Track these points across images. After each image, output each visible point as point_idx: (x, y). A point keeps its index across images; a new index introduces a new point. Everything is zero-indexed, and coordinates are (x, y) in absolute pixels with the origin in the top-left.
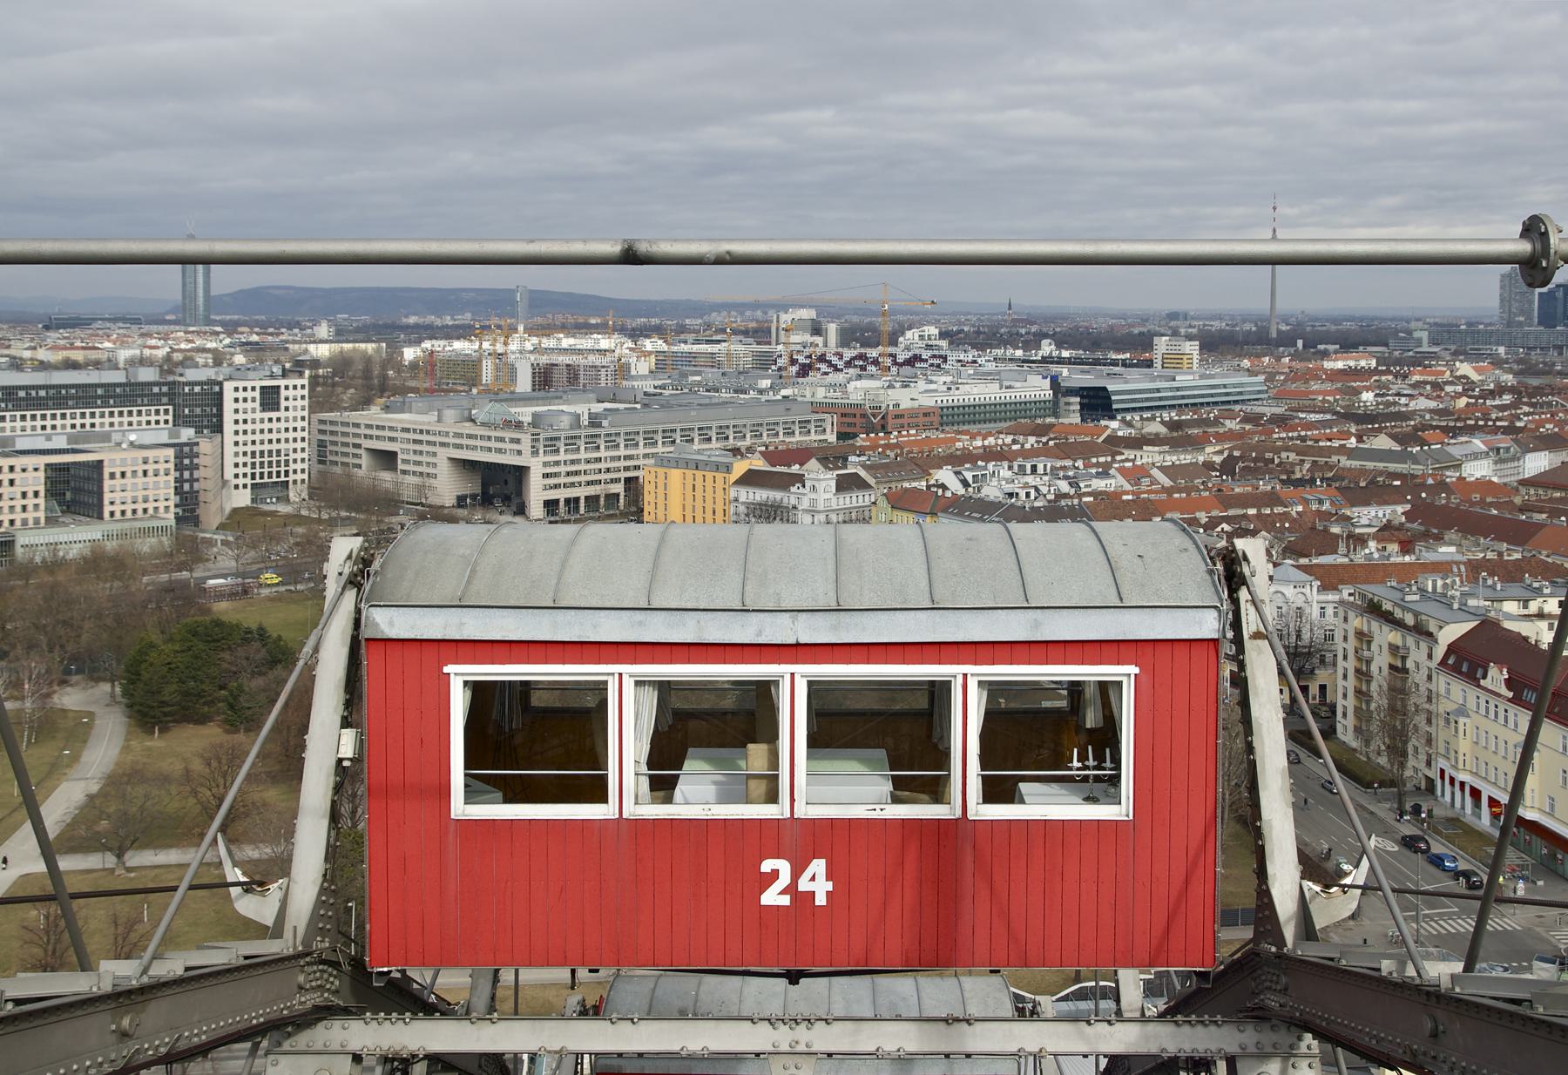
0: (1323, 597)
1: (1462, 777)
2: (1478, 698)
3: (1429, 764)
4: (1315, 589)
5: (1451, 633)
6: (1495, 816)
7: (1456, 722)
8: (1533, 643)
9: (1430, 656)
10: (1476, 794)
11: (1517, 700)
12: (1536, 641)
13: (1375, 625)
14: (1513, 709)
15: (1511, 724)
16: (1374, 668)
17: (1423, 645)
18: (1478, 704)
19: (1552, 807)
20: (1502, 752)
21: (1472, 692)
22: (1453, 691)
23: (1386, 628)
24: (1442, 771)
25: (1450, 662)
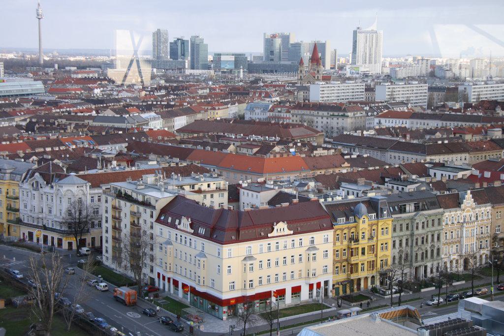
1: (167, 275)
2: (176, 235)
3: (152, 271)
4: (88, 187)
5: (160, 206)
6: (185, 293)
8: (201, 204)
9: (152, 216)
10: (176, 283)
11: (196, 234)
12: (203, 204)
13: (122, 203)
14: (194, 238)
15: (193, 246)
16: (122, 225)
17: (149, 211)
18: (176, 238)
19: (213, 284)
20: (188, 260)
21: (174, 232)
22: (162, 232)
23: (128, 204)
24: (159, 274)
25: (162, 218)
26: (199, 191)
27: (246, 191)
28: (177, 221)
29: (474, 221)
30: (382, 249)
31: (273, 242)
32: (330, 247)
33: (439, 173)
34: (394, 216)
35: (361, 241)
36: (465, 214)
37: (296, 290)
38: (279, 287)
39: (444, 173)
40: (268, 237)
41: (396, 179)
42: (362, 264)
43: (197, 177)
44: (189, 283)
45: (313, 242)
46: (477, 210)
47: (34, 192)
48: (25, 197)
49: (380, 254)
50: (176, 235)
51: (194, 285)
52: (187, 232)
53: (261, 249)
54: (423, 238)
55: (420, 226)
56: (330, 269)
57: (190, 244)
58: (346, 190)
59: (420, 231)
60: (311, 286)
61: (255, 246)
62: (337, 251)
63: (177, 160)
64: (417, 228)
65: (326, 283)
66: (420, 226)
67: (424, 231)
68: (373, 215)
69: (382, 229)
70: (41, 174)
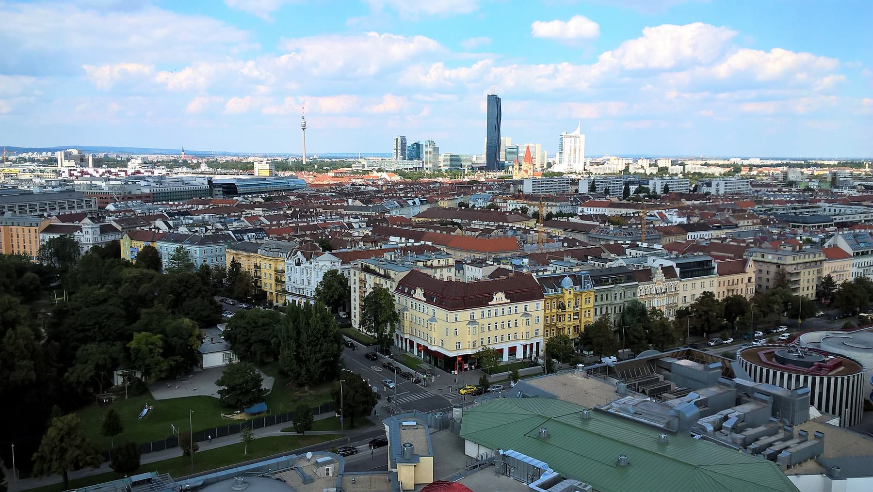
0: (343, 267)
2: (412, 302)
4: (340, 264)
6: (419, 351)
7: (403, 314)
11: (429, 301)
13: (368, 276)
14: (426, 305)
18: (412, 305)
19: (442, 344)
21: (410, 301)
23: (372, 277)
24: (397, 335)
26: (431, 267)
27: (470, 267)
28: (413, 291)
29: (664, 292)
30: (585, 315)
31: (493, 310)
32: (541, 314)
33: (634, 252)
34: (596, 288)
35: (567, 310)
36: (656, 287)
37: (513, 351)
38: (497, 347)
39: (638, 252)
40: (489, 305)
41: (598, 258)
42: (569, 329)
43: (429, 255)
44: (423, 343)
45: (526, 309)
46: (667, 283)
47: (297, 267)
48: (290, 271)
49: (584, 320)
50: (412, 302)
51: (426, 344)
52: (421, 300)
53: (483, 315)
54: (620, 307)
55: (618, 297)
56: (541, 332)
57: (424, 311)
58: (555, 266)
59: (618, 301)
60: (525, 347)
61: (477, 312)
62: (547, 317)
63: (412, 241)
64: (615, 298)
65: (538, 344)
66: (618, 297)
67: (622, 301)
68: (578, 286)
69: (586, 299)
70: (302, 252)
